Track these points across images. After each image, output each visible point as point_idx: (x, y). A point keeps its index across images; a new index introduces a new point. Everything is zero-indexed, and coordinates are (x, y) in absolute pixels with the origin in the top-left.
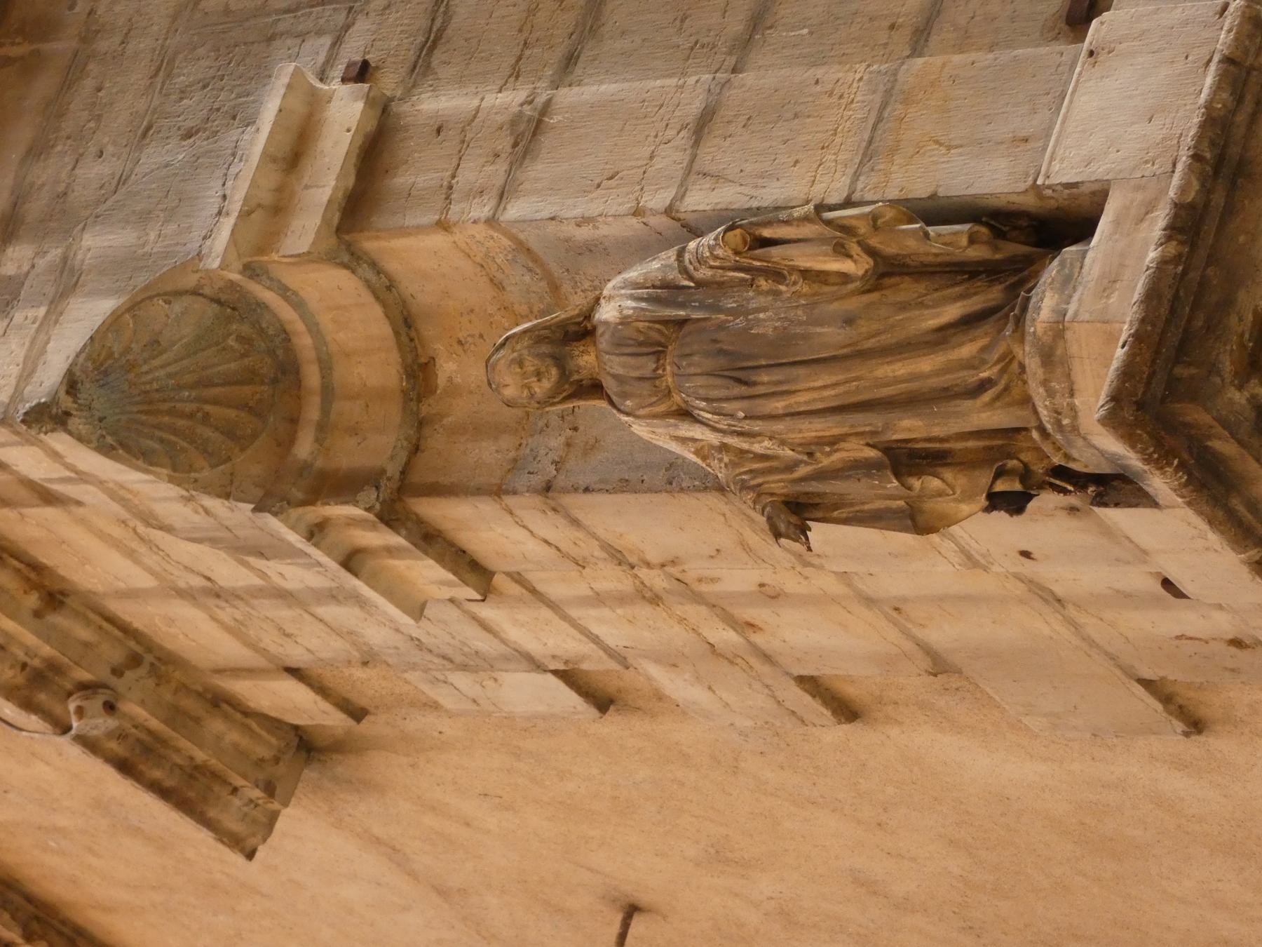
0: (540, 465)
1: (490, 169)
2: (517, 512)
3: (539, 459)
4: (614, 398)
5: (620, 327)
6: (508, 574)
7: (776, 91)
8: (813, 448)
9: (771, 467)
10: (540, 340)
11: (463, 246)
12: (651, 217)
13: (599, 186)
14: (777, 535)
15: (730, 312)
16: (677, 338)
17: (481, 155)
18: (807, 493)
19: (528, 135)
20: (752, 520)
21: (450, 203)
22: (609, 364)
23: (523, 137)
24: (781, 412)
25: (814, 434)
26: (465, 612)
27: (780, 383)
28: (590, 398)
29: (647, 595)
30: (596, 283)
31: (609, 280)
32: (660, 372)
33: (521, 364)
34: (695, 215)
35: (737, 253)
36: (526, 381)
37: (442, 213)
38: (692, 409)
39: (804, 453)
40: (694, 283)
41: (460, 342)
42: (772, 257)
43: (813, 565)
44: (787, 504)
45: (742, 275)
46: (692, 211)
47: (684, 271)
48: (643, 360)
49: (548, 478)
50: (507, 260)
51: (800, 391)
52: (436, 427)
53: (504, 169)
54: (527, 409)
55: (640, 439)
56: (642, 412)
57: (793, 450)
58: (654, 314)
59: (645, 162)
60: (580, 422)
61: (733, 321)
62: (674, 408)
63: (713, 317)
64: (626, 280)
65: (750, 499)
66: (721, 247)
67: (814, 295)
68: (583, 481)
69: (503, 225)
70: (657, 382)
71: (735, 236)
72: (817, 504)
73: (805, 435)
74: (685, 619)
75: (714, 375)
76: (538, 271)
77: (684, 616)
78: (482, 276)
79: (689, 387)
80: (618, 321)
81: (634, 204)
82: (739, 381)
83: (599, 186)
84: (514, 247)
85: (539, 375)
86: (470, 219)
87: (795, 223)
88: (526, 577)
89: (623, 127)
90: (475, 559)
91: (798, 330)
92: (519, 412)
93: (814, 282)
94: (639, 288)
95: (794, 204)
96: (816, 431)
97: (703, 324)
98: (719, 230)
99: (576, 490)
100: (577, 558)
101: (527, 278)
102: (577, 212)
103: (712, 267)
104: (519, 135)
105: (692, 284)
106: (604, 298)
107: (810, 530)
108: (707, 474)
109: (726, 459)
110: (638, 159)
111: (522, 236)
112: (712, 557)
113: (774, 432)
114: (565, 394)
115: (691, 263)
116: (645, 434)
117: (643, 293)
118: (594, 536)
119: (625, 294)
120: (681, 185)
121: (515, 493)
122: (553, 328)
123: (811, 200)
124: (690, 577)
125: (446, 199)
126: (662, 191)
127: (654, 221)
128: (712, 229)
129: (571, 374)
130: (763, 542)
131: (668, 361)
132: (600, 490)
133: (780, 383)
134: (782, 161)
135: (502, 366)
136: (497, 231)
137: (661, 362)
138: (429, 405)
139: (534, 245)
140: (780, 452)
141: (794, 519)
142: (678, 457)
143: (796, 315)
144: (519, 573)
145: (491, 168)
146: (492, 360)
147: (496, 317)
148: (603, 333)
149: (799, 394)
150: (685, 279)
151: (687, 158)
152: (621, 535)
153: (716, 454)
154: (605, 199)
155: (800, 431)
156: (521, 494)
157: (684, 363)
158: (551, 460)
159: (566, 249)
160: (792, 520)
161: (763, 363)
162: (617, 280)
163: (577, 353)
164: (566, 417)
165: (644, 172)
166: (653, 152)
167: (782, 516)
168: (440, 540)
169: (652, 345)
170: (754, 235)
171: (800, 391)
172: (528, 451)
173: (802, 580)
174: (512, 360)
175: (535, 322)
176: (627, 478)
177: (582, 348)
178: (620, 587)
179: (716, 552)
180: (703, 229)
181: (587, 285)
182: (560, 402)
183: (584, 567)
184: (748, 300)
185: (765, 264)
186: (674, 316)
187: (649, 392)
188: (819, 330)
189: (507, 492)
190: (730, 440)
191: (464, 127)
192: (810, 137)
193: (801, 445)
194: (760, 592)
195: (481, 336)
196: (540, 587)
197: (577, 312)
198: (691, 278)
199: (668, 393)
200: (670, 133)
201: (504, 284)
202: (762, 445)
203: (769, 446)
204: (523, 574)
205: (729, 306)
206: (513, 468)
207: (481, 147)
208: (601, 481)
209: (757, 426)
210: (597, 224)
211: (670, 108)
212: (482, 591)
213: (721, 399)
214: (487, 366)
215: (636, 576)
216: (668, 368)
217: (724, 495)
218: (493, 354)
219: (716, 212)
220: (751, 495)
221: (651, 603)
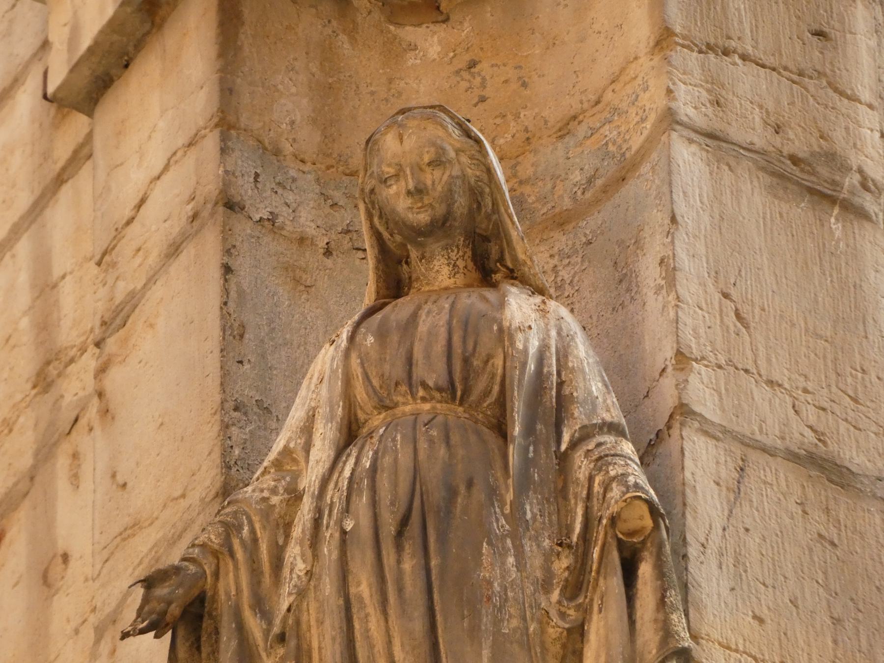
0: (269, 192)
1: (757, 117)
2: (193, 154)
3: (280, 191)
4: (378, 316)
5: (495, 328)
6: (89, 137)
7: (878, 588)
8: (293, 643)
9: (262, 572)
10: (475, 195)
11: (631, 72)
12: (674, 382)
13: (726, 296)
14: (149, 583)
15: (518, 506)
16: (476, 422)
17: (779, 103)
18: (217, 632)
19: (809, 180)
20: (174, 541)
21: (700, 52)
22: (435, 309)
23: (808, 173)
24: (353, 590)
25: (315, 644)
26: (26, 67)
27: (400, 590)
28: (378, 278)
29: (51, 367)
30: (568, 290)
31: (572, 311)
32: (421, 393)
33: (437, 163)
34: (676, 454)
35: (614, 520)
36: (408, 172)
37: (684, 38)
38: (359, 445)
39: (284, 627)
40: (567, 449)
41: (472, 64)
42: (605, 578)
43: (98, 641)
44: (201, 599)
45: (578, 528)
46: (682, 448)
47: (586, 434)
48: (441, 365)
49: (247, 204)
50: (607, 144)
51: (387, 621)
52: (334, 23)
53: (756, 140)
54: (361, 174)
55: (310, 359)
56: (355, 361)
57: (289, 610)
58: (516, 383)
59: (763, 372)
60: (340, 260)
61: (503, 514)
62: (361, 416)
63: (510, 481)
64: (573, 339)
65: (210, 539)
66: (624, 494)
67: (543, 644)
68: (243, 265)
69: (664, 138)
70: (404, 388)
71: (641, 518)
72: (199, 649)
73: (314, 631)
74: (11, 431)
75: (415, 478)
76: (588, 195)
77: (16, 429)
78: (581, 102)
79: (394, 440)
80: (506, 324)
81: (696, 353)
82: (404, 521)
83: (726, 296)
84: (628, 155)
85: (418, 192)
86: (674, 84)
87: (661, 616)
88: (84, 167)
89: (821, 337)
90: (116, 83)
91: (486, 621)
92: (357, 160)
93: (564, 646)
94: (558, 360)
95: (691, 615)
96: (320, 648)
97: (498, 464)
98: (652, 492)
99: (228, 252)
100: (114, 253)
101: (577, 176)
102: (684, 260)
103: (591, 479)
104: (810, 165)
105: (563, 447)
106: (544, 302)
107: (156, 637)
108: (251, 469)
109: (275, 500)
110: (769, 361)
111: (645, 168)
112: (114, 476)
113: (320, 579)
114: (386, 235)
115: (599, 445)
116: (319, 367)
117: (550, 366)
118: (152, 280)
119: (549, 336)
120: (725, 431)
121: (224, 151)
122: (495, 217)
123: (698, 643)
124: (81, 439)
125: (708, 46)
126: (716, 398)
127: (668, 386)
128: (652, 481)
129: (420, 245)
130: (137, 561)
131: (439, 406)
132: (226, 291)
133: (400, 590)
134: (763, 597)
135: (432, 131)
136: (655, 126)
137: (437, 395)
138: (370, 13)
139: (629, 189)
140: (286, 589)
141: (175, 610)
142: (280, 421)
143: (510, 616)
144: (90, 156)
145: (757, 119)
146: (443, 115)
147: (512, 124)
148: (486, 300)
149: (382, 623)
150: (573, 436)
151: (768, 441)
152: (151, 326)
153: (283, 483)
154: (704, 306)
155: (320, 623)
156: (222, 162)
157: (434, 433)
158: (276, 211)
159: (623, 241)
160: (173, 606)
161: (434, 563)
162: (572, 324)
163: (453, 255)
164: (348, 237)
165: (746, 371)
166: (780, 385)
167: (180, 591)
168: (147, 26)
169: (466, 379)
170: (641, 550)
171: (387, 621)
172: (292, 173)
173: (73, 624)
174: (443, 149)
175: (505, 188)
176: (247, 336)
177: (461, 264)
178: (66, 324)
179: (121, 482)
180: (654, 467)
181: (565, 274)
182: (372, 227)
183: (99, 264)
184: (536, 539)
185: (594, 567)
186: (513, 417)
187: (387, 374)
188: (486, 653)
189: (224, 138)
190: (307, 506)
191: (825, 75)
192: (801, 642)
193: (298, 623)
194: (54, 556)
195: (483, 99)
196: (66, 191)
197: (521, 256)
198: (574, 445)
199: (384, 406)
200: (811, 415)
201: (567, 139)
202: (299, 558)
203: (296, 570)
204: (89, 165)
205: (528, 507)
206: (265, 149)
207: (792, 103)
208: (241, 293)
209: (329, 551)
210: (664, 292)
211: (851, 413)
212: (59, 95)
213: (375, 492)
214: (432, 107)
215: (83, 350)
216: (427, 406)
217: (217, 495)
218: (453, 117)
219: (679, 488)
220: (214, 539)
221: (38, 375)
